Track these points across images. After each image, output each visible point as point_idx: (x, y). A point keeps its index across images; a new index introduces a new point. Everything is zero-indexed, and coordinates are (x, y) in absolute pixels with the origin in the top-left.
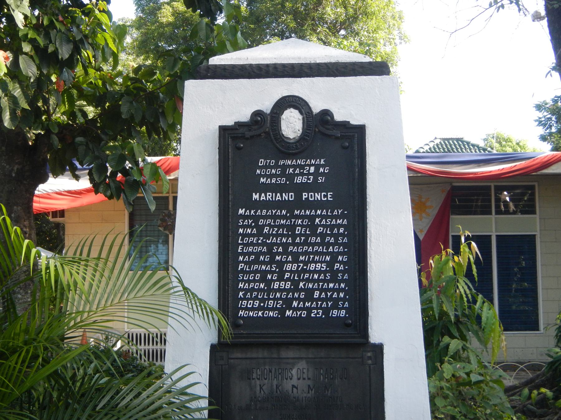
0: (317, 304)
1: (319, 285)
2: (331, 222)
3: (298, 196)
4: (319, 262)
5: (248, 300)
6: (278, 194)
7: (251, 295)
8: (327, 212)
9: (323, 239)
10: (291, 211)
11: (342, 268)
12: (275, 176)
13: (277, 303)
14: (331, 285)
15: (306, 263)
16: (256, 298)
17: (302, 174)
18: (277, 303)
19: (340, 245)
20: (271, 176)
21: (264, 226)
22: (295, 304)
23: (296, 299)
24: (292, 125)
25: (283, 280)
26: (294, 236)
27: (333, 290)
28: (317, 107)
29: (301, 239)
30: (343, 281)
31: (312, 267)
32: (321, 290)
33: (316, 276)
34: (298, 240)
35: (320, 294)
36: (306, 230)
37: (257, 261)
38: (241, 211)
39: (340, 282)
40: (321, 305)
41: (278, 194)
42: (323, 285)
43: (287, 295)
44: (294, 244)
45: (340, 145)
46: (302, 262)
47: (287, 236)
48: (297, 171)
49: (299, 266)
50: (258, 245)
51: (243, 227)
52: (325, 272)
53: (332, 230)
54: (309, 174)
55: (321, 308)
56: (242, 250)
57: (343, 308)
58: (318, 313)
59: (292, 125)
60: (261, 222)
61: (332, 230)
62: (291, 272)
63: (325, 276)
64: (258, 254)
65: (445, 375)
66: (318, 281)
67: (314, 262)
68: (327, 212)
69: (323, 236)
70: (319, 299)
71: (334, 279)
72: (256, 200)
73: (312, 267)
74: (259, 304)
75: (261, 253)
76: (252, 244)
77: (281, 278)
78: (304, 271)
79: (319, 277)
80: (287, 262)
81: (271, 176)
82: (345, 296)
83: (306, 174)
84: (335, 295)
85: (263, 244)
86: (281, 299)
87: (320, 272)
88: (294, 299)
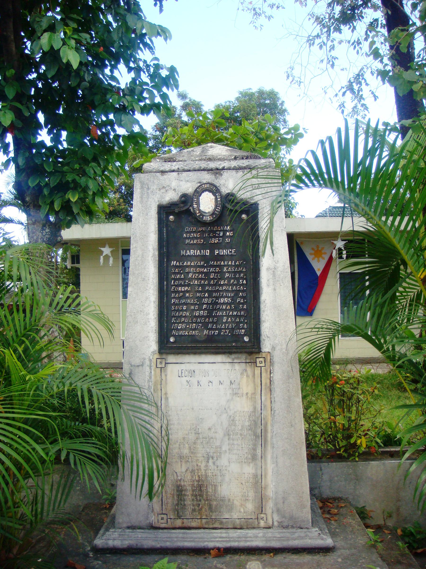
0: (225, 326)
1: (226, 313)
2: (234, 269)
3: (212, 252)
4: (226, 297)
5: (178, 323)
6: (198, 251)
7: (181, 320)
8: (232, 263)
9: (229, 282)
10: (207, 262)
11: (242, 301)
12: (196, 238)
13: (198, 326)
14: (235, 313)
15: (217, 298)
16: (184, 322)
17: (215, 237)
18: (198, 326)
19: (241, 285)
20: (193, 238)
21: (188, 273)
22: (210, 326)
23: (211, 323)
24: (207, 204)
25: (202, 310)
26: (210, 280)
27: (237, 316)
28: (225, 191)
29: (214, 282)
30: (243, 309)
31: (222, 300)
32: (228, 316)
33: (224, 307)
34: (212, 282)
35: (227, 319)
36: (217, 275)
37: (183, 297)
38: (174, 263)
39: (240, 310)
40: (228, 326)
41: (198, 251)
42: (229, 313)
43: (205, 320)
44: (209, 285)
45: (239, 215)
46: (214, 297)
47: (205, 279)
48: (211, 235)
49: (213, 300)
50: (185, 286)
51: (175, 273)
52: (230, 304)
53: (235, 275)
54: (219, 237)
55: (228, 328)
56: (174, 289)
57: (243, 328)
58: (226, 332)
59: (207, 204)
60: (187, 270)
61: (235, 275)
62: (207, 304)
63: (231, 307)
64: (185, 292)
65: (309, 410)
66: (226, 310)
67: (222, 297)
68: (232, 263)
69: (229, 279)
70: (226, 322)
71: (236, 309)
72: (183, 255)
73: (222, 300)
74: (186, 326)
75: (187, 291)
76: (181, 285)
77: (200, 309)
78: (217, 303)
79: (226, 307)
80: (205, 297)
81: (193, 238)
82: (244, 320)
83: (217, 237)
84: (238, 320)
85: (188, 285)
86: (200, 322)
87: (227, 304)
88: (209, 322)
